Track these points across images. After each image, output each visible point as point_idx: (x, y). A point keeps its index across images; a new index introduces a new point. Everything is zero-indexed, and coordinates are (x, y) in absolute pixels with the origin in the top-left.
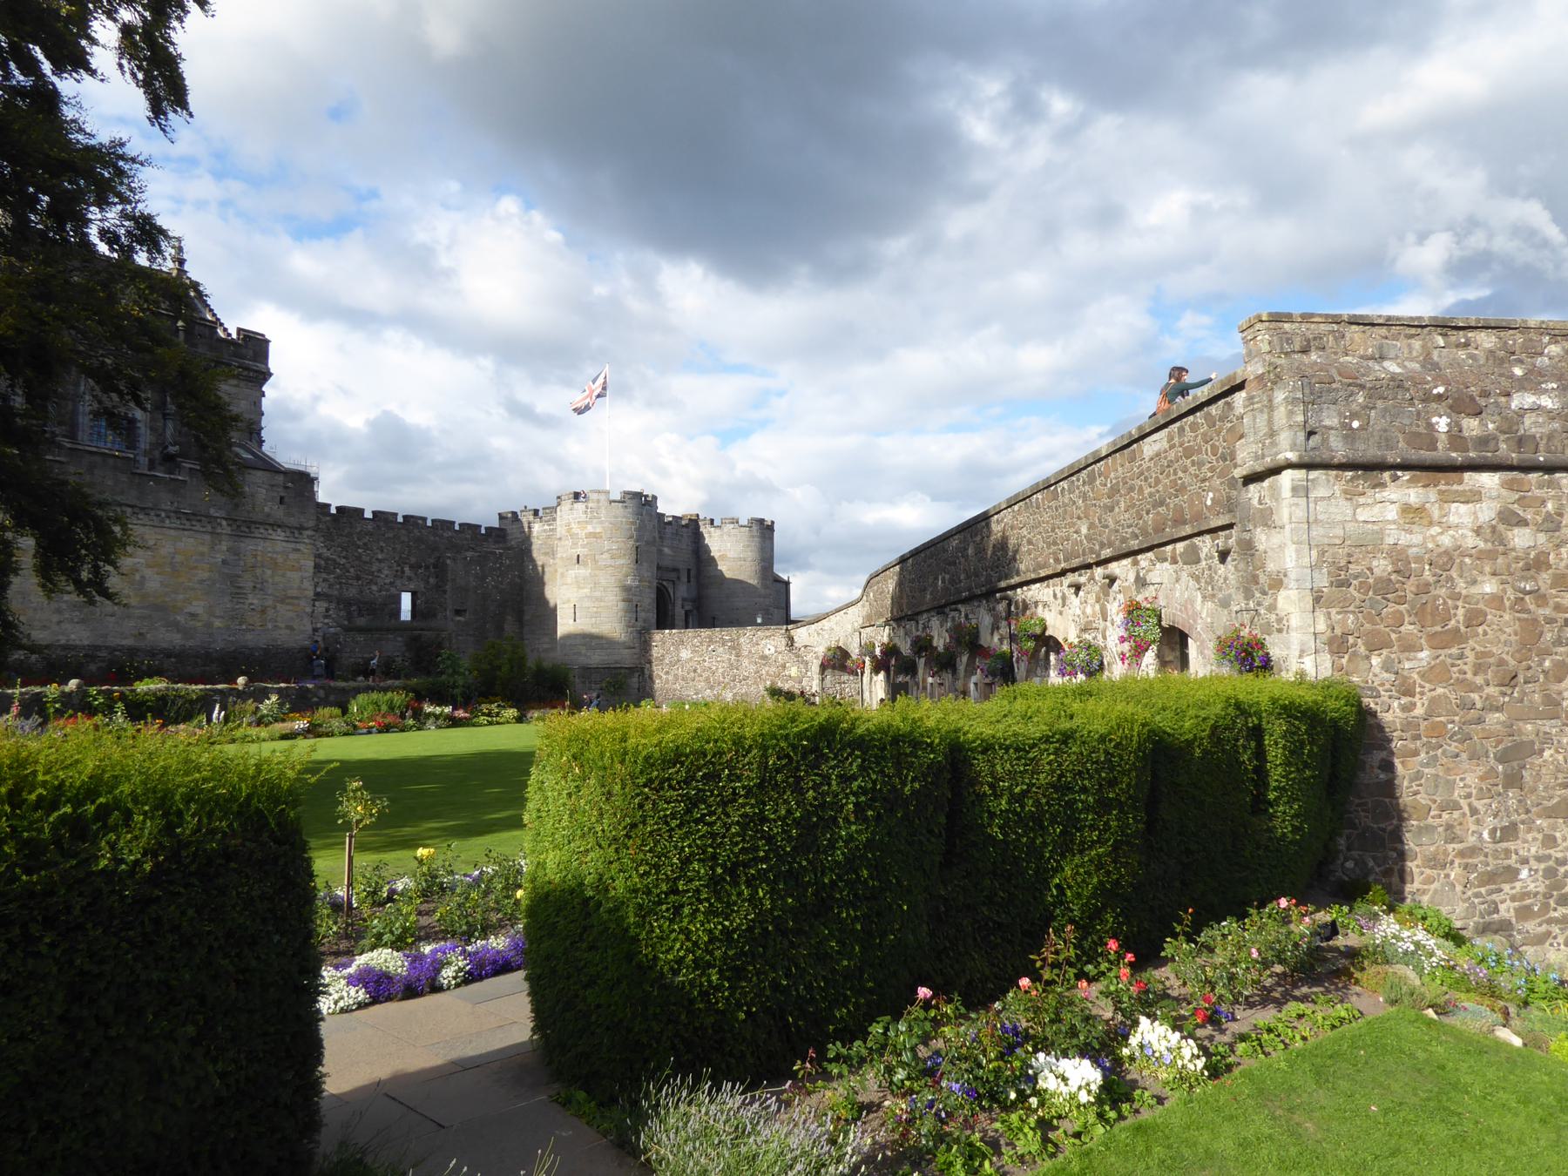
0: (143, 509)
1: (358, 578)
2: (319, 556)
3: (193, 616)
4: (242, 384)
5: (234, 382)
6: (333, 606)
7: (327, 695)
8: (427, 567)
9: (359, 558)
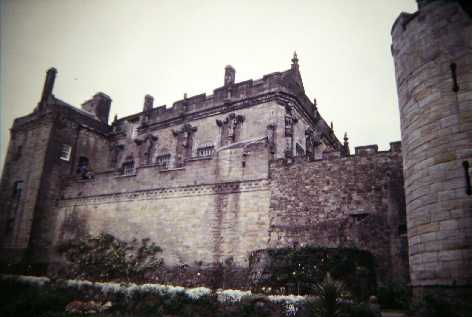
0: (163, 189)
1: (307, 210)
2: (275, 198)
3: (188, 247)
4: (266, 105)
5: (262, 105)
6: (284, 234)
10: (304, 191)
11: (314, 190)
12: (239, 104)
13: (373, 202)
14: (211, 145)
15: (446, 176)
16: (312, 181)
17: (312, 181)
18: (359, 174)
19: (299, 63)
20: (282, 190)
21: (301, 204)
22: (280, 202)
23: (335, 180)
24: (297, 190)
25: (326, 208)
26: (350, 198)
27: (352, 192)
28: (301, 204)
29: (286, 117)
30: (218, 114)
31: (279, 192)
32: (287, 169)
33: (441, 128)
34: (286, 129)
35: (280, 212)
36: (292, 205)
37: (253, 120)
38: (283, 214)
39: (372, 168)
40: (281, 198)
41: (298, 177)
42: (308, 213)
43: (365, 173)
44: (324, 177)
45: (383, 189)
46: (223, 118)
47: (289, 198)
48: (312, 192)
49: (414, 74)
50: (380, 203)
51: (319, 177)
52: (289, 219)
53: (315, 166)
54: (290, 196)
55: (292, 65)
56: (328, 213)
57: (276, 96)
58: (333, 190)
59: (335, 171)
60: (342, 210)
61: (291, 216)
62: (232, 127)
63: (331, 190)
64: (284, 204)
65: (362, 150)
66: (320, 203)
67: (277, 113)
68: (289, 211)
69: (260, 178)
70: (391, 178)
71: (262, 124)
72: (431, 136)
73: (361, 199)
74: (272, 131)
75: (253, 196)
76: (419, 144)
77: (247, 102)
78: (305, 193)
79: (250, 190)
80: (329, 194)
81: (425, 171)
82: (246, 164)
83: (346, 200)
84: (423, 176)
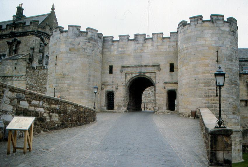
2: (28, 84)
4: (31, 36)
5: (29, 36)
9: (41, 83)
12: (18, 34)
14: (4, 54)
17: (43, 78)
19: (55, 11)
21: (38, 87)
22: (30, 86)
24: (37, 81)
28: (38, 87)
29: (40, 43)
30: (8, 38)
32: (34, 72)
34: (40, 49)
36: (34, 88)
37: (25, 44)
40: (31, 85)
41: (38, 76)
46: (11, 40)
47: (34, 85)
54: (34, 84)
55: (51, 11)
57: (35, 33)
62: (15, 46)
64: (32, 87)
67: (35, 41)
69: (22, 75)
71: (28, 46)
74: (32, 51)
75: (19, 83)
77: (22, 34)
78: (40, 83)
79: (18, 80)
82: (16, 68)
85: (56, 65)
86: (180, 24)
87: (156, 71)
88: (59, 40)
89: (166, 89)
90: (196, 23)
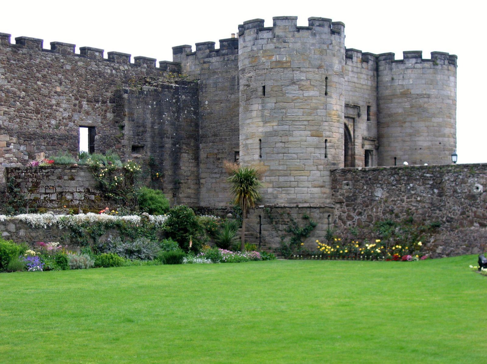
1: (38, 112)
6: (15, 140)
7: (18, 229)
8: (104, 102)
10: (35, 86)
11: (45, 89)
13: (99, 115)
15: (317, 145)
16: (44, 76)
17: (44, 76)
18: (89, 80)
20: (9, 80)
21: (31, 103)
23: (67, 81)
24: (27, 84)
25: (57, 113)
26: (81, 107)
27: (83, 99)
28: (31, 103)
31: (6, 83)
33: (317, 115)
35: (7, 109)
38: (12, 113)
39: (100, 77)
40: (8, 91)
42: (39, 116)
43: (95, 81)
44: (57, 75)
45: (108, 102)
47: (18, 93)
48: (44, 91)
49: (301, 69)
50: (105, 117)
51: (51, 73)
52: (18, 120)
53: (47, 58)
54: (19, 90)
56: (60, 120)
58: (65, 93)
59: (68, 70)
60: (73, 119)
61: (21, 117)
63: (63, 92)
65: (92, 52)
66: (51, 106)
68: (18, 110)
70: (129, 97)
72: (309, 118)
73: (90, 109)
76: (300, 119)
80: (61, 97)
81: (304, 138)
83: (77, 107)
84: (301, 141)
85: (326, 94)
86: (413, 54)
87: (355, 117)
88: (330, 47)
89: (365, 148)
90: (443, 63)
